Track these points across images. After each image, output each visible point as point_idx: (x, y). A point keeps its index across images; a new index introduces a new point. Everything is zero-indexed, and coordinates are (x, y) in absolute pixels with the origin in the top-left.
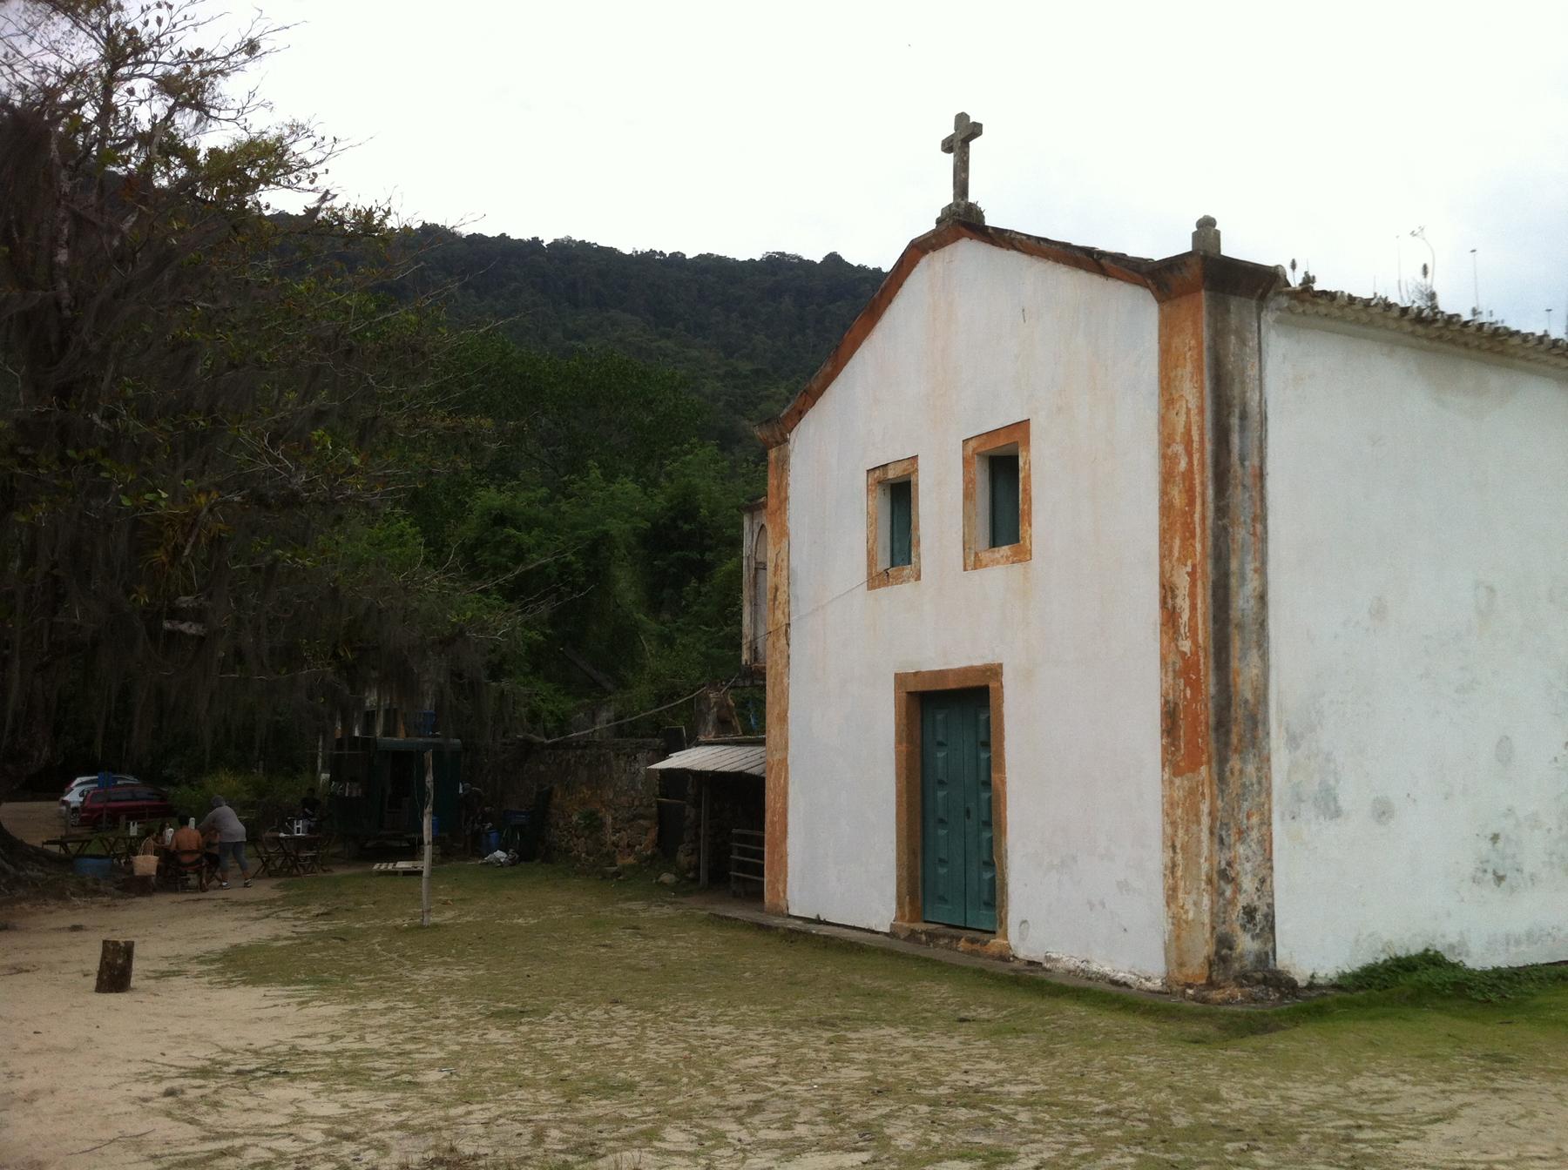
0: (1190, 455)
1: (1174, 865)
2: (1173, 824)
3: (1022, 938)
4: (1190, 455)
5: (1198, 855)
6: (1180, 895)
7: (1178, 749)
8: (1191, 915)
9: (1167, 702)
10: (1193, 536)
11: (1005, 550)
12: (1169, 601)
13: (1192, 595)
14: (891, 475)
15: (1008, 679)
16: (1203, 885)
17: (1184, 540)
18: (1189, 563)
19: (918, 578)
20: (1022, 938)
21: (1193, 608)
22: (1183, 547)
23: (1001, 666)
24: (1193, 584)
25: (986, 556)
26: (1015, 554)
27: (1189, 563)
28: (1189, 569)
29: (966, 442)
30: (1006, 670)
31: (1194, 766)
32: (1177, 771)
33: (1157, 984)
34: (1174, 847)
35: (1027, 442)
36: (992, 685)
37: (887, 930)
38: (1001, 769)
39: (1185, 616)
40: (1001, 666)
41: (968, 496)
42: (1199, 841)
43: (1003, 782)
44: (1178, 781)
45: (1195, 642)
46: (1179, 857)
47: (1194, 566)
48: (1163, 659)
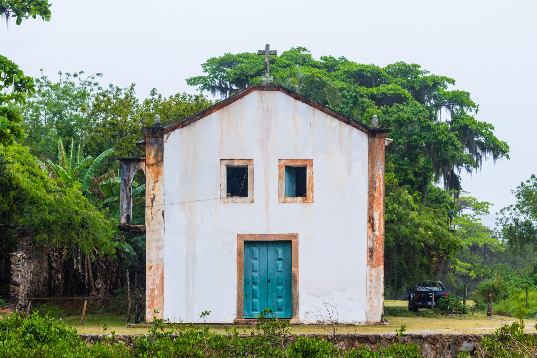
0: (380, 183)
1: (371, 292)
2: (371, 281)
3: (306, 317)
4: (380, 183)
5: (379, 289)
6: (373, 299)
7: (373, 261)
8: (376, 304)
9: (370, 248)
10: (380, 204)
11: (300, 199)
12: (371, 221)
13: (380, 220)
14: (236, 163)
15: (300, 238)
16: (381, 296)
17: (377, 205)
18: (379, 211)
19: (253, 202)
20: (306, 317)
21: (380, 224)
22: (376, 206)
23: (297, 234)
24: (380, 217)
25: (289, 199)
26: (304, 200)
27: (379, 211)
28: (379, 213)
29: (280, 160)
30: (299, 235)
31: (379, 265)
32: (373, 267)
33: (363, 324)
34: (371, 287)
35: (312, 166)
36: (293, 241)
37: (231, 322)
38: (297, 266)
39: (377, 226)
40: (297, 234)
41: (280, 177)
42: (380, 285)
43: (298, 271)
44: (373, 269)
45: (380, 232)
46: (373, 290)
47: (380, 212)
48: (368, 237)
